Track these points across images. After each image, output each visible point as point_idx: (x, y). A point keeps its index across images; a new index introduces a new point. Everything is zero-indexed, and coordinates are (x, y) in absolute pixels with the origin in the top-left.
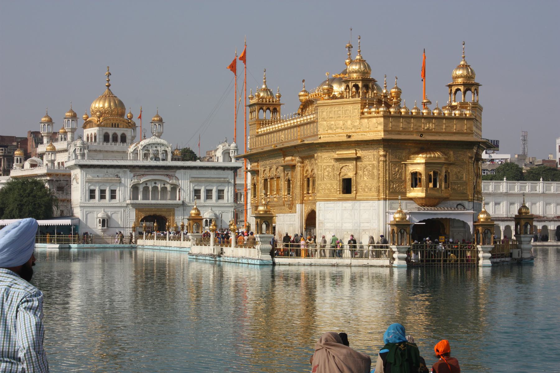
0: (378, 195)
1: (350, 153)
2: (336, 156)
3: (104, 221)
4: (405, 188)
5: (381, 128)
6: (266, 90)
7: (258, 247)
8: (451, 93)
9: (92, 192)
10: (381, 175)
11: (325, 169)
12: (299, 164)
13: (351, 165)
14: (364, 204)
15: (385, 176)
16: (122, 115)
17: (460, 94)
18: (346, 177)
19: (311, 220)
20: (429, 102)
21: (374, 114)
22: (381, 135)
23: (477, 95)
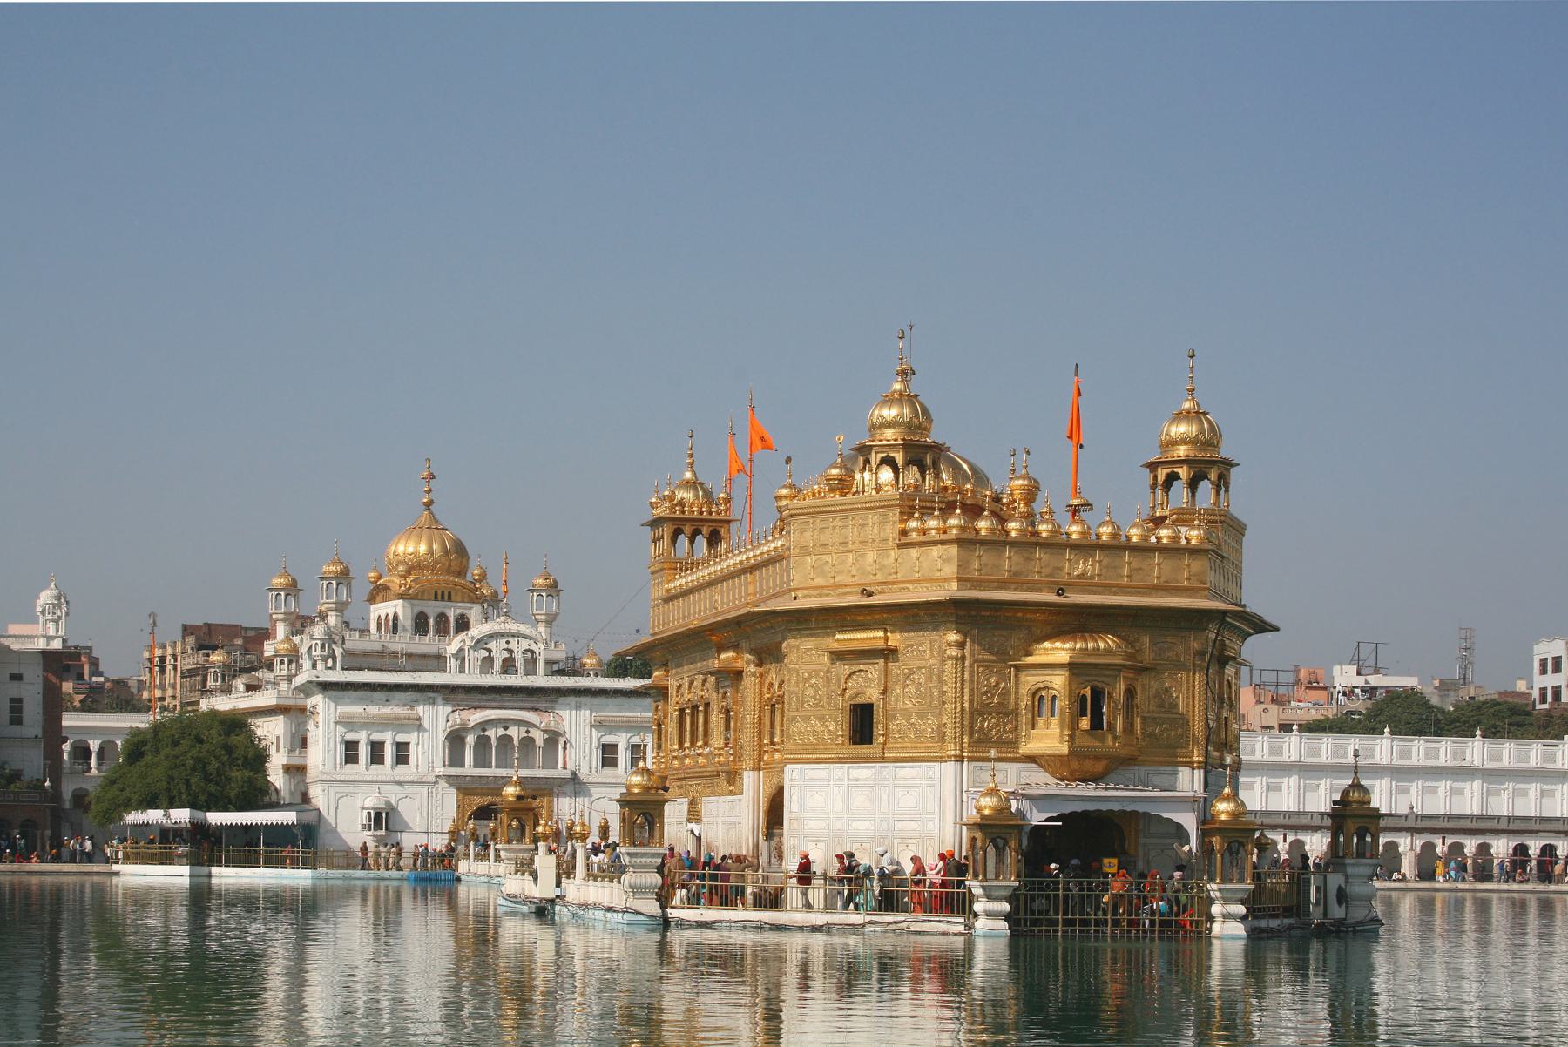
1: (872, 638)
2: (835, 646)
3: (378, 815)
5: (951, 570)
6: (694, 484)
7: (626, 879)
8: (1154, 486)
11: (806, 680)
12: (752, 669)
13: (874, 670)
14: (907, 771)
16: (462, 573)
17: (1180, 491)
18: (860, 700)
19: (774, 814)
20: (1088, 505)
22: (952, 590)
23: (1227, 491)
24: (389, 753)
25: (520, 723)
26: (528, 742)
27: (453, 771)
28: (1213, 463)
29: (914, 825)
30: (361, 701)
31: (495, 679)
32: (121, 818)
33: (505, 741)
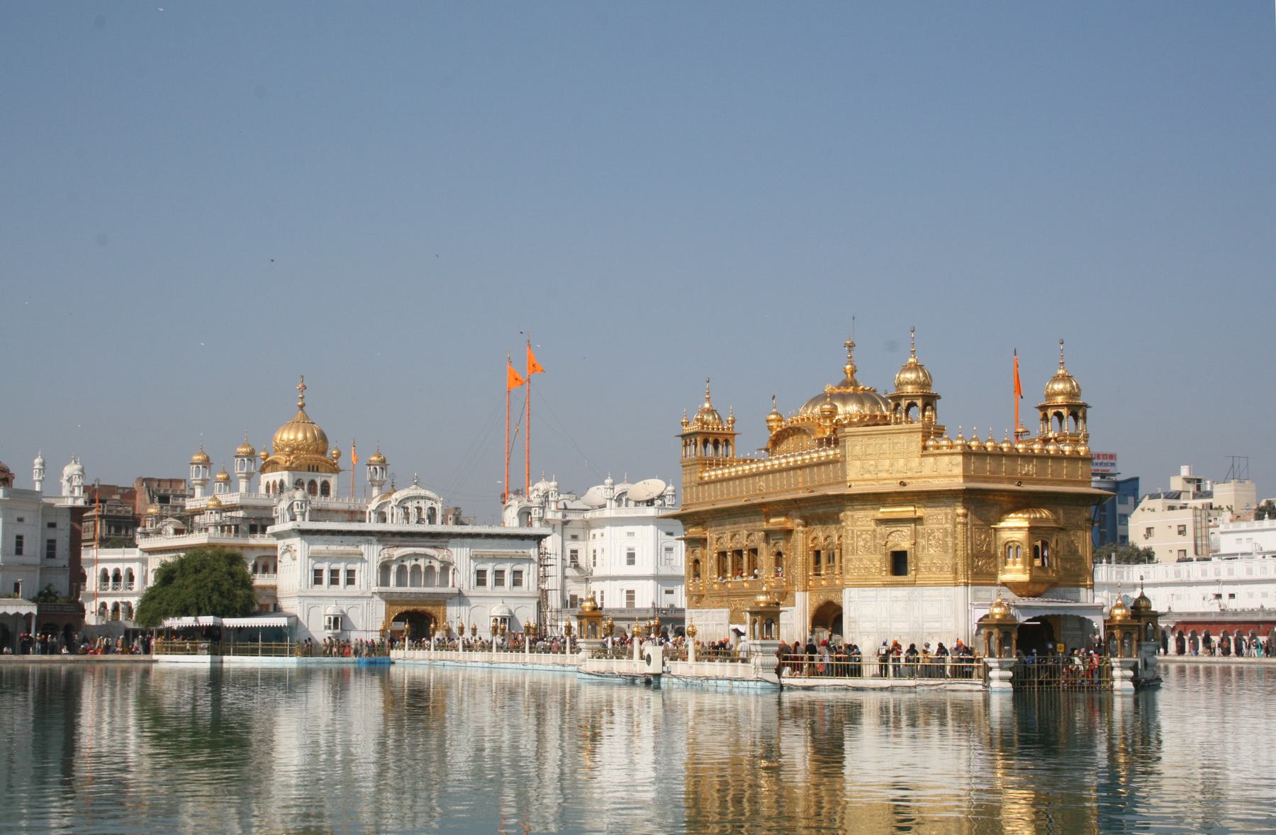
0: (955, 579)
1: (907, 511)
2: (880, 516)
3: (336, 619)
4: (996, 566)
5: (958, 470)
6: (711, 411)
9: (318, 573)
10: (960, 546)
11: (858, 536)
12: (801, 528)
13: (906, 530)
14: (928, 591)
15: (965, 548)
16: (324, 453)
21: (945, 450)
22: (958, 483)
24: (342, 577)
25: (425, 556)
26: (430, 569)
27: (384, 589)
28: (1080, 406)
29: (937, 625)
30: (325, 542)
31: (426, 527)
32: (160, 623)
33: (416, 568)
